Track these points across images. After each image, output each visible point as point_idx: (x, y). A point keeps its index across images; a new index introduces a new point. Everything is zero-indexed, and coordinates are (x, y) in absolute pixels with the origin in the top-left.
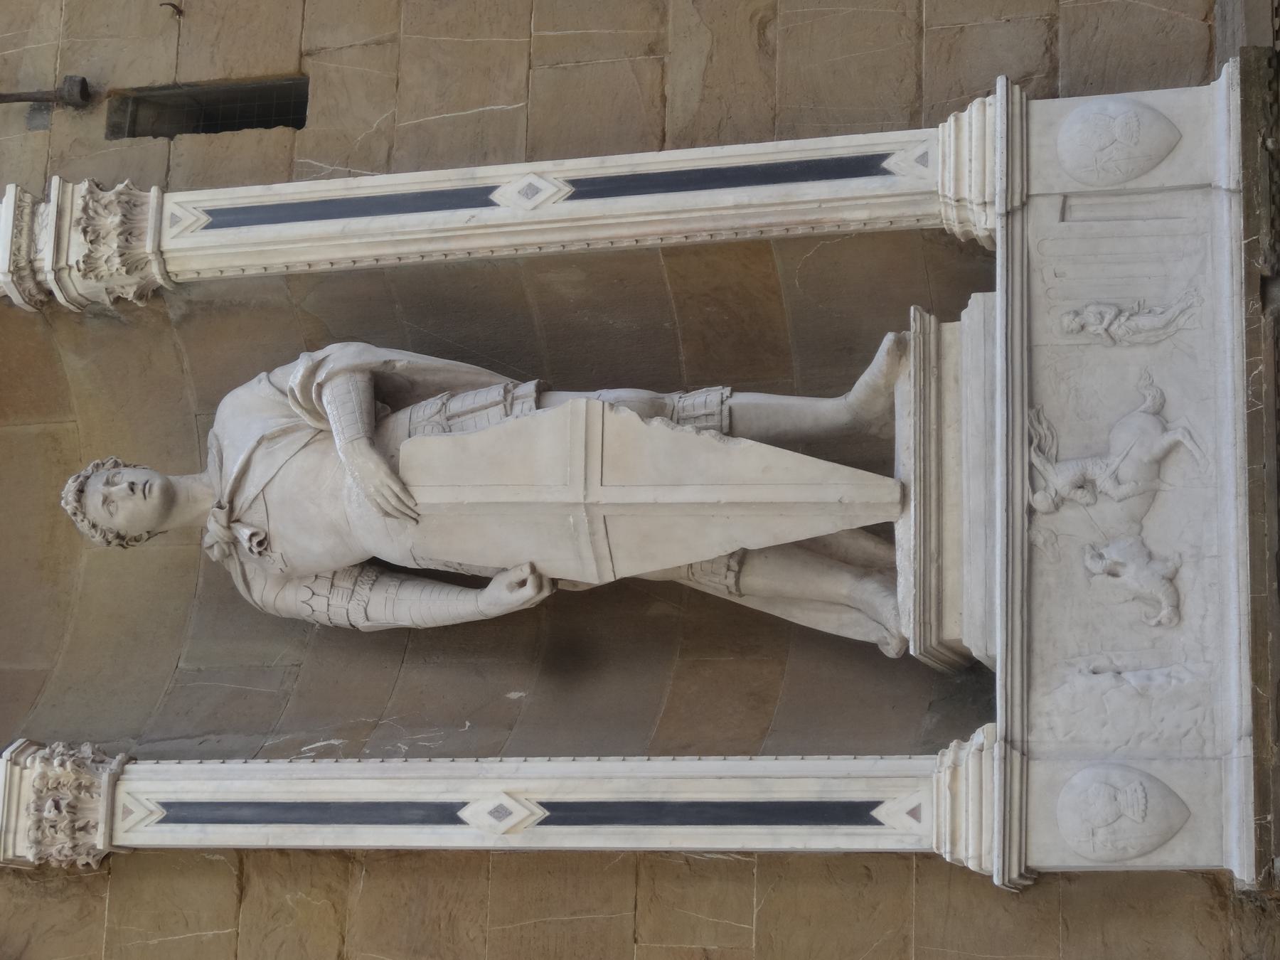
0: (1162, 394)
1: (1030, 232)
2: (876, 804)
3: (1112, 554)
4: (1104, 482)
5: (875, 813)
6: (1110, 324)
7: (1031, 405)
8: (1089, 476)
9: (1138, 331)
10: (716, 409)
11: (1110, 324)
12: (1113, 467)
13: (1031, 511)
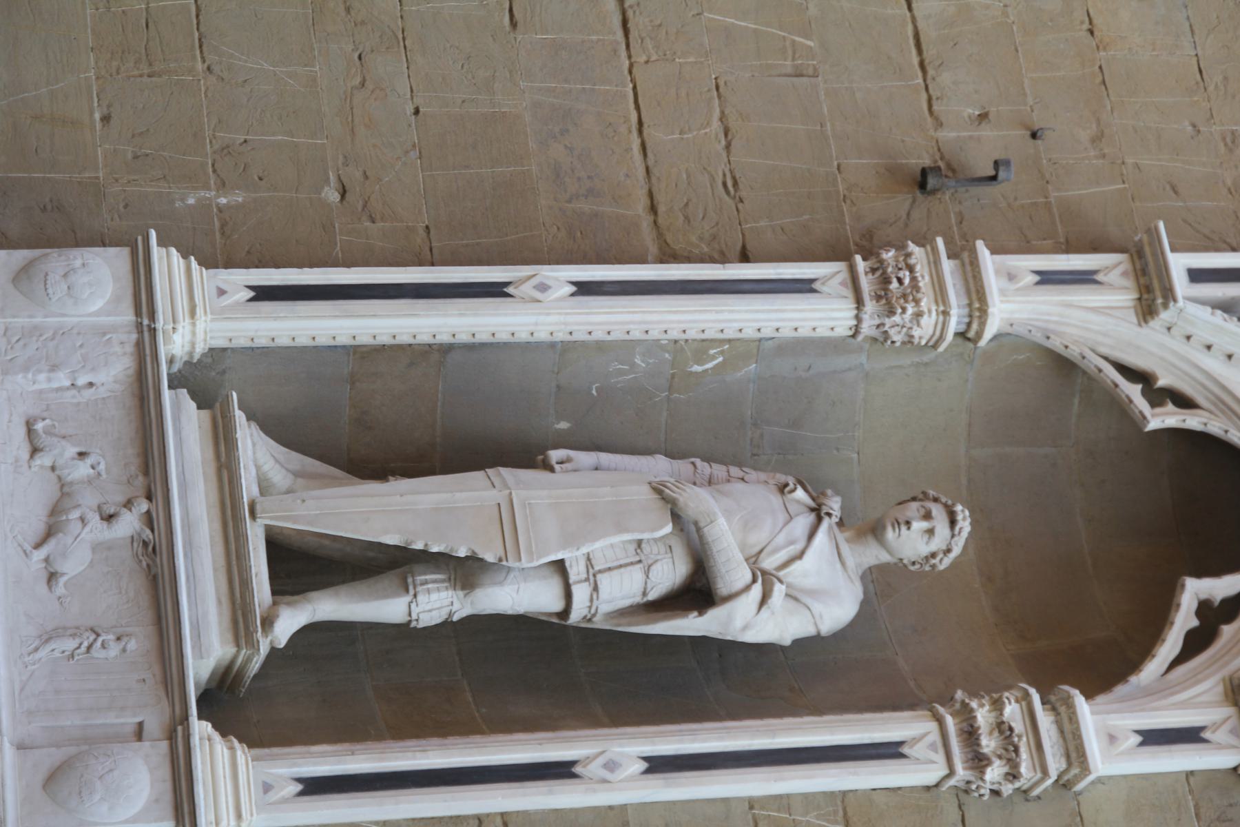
0: (50, 588)
1: (167, 710)
2: (251, 300)
3: (82, 470)
4: (94, 519)
5: (252, 294)
6: (95, 640)
7: (155, 578)
8: (105, 524)
9: (73, 636)
10: (419, 588)
11: (95, 640)
12: (87, 529)
13: (149, 498)
